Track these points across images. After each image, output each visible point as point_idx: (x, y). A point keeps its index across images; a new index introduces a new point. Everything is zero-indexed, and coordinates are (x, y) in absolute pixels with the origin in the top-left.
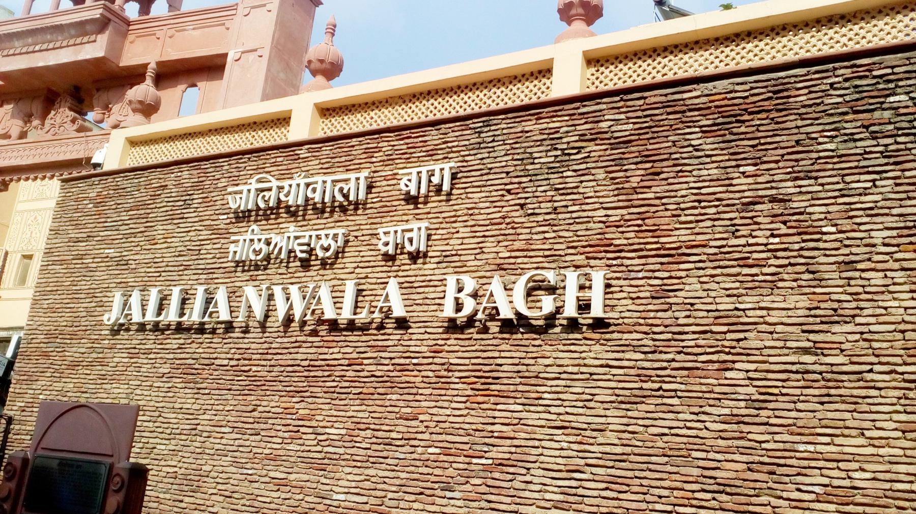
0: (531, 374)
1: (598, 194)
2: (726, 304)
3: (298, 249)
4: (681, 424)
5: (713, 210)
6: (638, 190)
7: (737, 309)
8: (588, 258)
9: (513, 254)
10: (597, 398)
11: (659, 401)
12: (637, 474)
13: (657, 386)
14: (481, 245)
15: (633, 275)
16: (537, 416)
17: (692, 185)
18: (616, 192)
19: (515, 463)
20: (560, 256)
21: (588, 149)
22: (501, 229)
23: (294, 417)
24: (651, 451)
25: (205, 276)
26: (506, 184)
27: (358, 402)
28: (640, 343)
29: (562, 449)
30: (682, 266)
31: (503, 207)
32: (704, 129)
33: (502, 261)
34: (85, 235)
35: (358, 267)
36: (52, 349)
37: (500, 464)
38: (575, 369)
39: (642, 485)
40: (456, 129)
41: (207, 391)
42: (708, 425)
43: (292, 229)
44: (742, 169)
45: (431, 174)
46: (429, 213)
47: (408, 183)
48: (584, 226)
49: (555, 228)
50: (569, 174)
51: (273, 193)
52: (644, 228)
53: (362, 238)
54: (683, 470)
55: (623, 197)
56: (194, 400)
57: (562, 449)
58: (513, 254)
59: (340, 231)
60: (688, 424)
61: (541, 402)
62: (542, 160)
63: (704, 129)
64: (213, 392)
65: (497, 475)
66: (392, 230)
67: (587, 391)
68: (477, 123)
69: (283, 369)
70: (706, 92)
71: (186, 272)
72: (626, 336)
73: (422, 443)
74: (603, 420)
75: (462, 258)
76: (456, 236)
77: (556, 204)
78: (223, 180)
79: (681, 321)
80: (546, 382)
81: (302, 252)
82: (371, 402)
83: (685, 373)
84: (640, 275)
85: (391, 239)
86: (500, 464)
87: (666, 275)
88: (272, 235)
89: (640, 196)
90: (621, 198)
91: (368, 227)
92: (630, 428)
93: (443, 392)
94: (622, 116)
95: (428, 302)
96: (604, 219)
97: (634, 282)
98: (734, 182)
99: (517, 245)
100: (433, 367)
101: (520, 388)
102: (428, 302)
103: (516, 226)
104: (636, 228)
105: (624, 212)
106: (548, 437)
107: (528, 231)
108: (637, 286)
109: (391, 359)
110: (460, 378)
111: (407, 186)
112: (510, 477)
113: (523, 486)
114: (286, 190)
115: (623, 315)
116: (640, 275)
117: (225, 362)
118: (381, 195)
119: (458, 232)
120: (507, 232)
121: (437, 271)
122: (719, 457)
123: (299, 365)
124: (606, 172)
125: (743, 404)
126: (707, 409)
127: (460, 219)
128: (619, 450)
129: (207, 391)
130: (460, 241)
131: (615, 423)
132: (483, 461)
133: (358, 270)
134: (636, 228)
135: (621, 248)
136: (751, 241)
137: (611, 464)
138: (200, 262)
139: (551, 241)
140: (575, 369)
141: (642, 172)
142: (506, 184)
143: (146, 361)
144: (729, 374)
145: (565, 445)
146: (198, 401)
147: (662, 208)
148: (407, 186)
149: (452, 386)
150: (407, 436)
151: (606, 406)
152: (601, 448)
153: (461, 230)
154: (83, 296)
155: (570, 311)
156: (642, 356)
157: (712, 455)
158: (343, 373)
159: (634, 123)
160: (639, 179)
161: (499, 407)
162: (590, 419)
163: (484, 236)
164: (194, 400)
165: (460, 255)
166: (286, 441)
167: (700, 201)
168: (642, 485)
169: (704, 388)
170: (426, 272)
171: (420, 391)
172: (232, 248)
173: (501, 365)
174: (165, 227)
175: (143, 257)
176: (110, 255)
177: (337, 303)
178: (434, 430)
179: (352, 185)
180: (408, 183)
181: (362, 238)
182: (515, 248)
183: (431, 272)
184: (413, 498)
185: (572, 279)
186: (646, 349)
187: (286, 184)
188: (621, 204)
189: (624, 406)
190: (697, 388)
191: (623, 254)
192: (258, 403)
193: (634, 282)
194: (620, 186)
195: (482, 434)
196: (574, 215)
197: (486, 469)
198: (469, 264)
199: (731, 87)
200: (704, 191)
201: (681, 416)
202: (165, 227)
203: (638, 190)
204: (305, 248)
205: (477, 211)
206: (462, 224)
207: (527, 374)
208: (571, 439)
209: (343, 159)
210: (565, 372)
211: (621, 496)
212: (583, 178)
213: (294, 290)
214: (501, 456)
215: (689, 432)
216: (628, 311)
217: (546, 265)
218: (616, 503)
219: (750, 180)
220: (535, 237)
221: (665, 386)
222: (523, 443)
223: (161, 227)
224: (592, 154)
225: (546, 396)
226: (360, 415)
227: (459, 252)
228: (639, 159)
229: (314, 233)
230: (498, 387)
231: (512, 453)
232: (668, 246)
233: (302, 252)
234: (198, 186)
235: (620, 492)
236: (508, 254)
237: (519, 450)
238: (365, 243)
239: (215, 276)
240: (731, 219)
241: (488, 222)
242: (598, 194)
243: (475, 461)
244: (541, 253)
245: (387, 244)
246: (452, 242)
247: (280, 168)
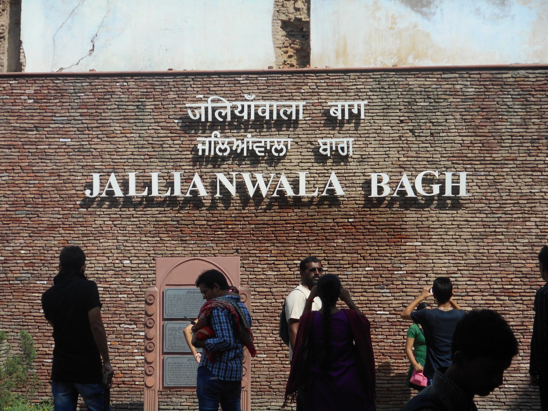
0: (425, 226)
1: (457, 127)
2: (526, 190)
3: (257, 150)
4: (505, 248)
5: (519, 141)
6: (479, 127)
7: (531, 192)
8: (453, 163)
9: (409, 159)
10: (462, 237)
11: (494, 237)
12: (485, 272)
13: (493, 230)
14: (387, 152)
15: (478, 173)
16: (430, 247)
17: (508, 127)
18: (467, 127)
19: (419, 272)
20: (437, 161)
21: (450, 100)
22: (399, 144)
23: (269, 255)
24: (491, 261)
25: (172, 164)
26: (400, 117)
27: (313, 245)
28: (484, 208)
29: (445, 263)
30: (504, 170)
31: (399, 130)
32: (514, 96)
33: (402, 163)
34: (33, 126)
35: (301, 162)
36: (23, 216)
37: (411, 273)
38: (450, 223)
39: (487, 277)
40: (362, 77)
41: (192, 242)
42: (518, 247)
43: (249, 137)
44: (532, 121)
46: (349, 130)
47: (336, 112)
48: (450, 145)
49: (433, 145)
50: (439, 114)
51: (229, 111)
52: (483, 148)
53: (301, 143)
54: (507, 269)
55: (472, 131)
56: (183, 248)
57: (445, 263)
58: (409, 159)
59: (290, 140)
60: (509, 248)
61: (432, 240)
62: (422, 104)
63: (514, 96)
64: (198, 242)
65: (409, 279)
66: (328, 141)
67: (457, 233)
68: (377, 75)
69: (253, 226)
70: (514, 76)
71: (152, 160)
72: (476, 205)
73: (362, 265)
74: (466, 248)
75: (375, 160)
76: (370, 146)
77: (433, 131)
78: (172, 93)
79: (504, 198)
80: (433, 230)
81: (260, 152)
82: (324, 244)
83: (507, 223)
84: (482, 173)
85: (328, 147)
86: (411, 273)
87: (496, 174)
88: (234, 139)
89: (481, 131)
90: (470, 130)
91: (305, 136)
92: (480, 251)
93: (372, 237)
94: (469, 83)
95: (356, 185)
96: (461, 142)
97: (479, 177)
98: (529, 127)
99: (410, 154)
100: (364, 224)
101: (419, 233)
102: (356, 185)
103: (409, 142)
104: (479, 148)
105: (472, 138)
106: (437, 258)
107: (416, 146)
108: (481, 180)
109: (333, 219)
110: (382, 229)
111: (335, 113)
112: (418, 279)
113: (425, 283)
114: (240, 108)
115: (474, 194)
116: (482, 173)
117: (204, 222)
118: (312, 115)
119: (371, 144)
120: (403, 146)
121: (359, 167)
122: (523, 262)
123: (267, 224)
124: (460, 115)
125: (534, 237)
126: (518, 240)
127: (371, 135)
128: (475, 262)
129: (192, 242)
130: (372, 150)
131: (472, 249)
132: (401, 272)
133: (301, 164)
134: (479, 148)
135: (472, 158)
136: (538, 158)
137: (471, 268)
138: (166, 153)
139: (431, 152)
140: (450, 223)
141: (481, 117)
142: (400, 117)
143: (128, 223)
144: (528, 223)
145: (447, 261)
146: (186, 249)
147: (492, 138)
148: (335, 113)
149: (377, 234)
150: (351, 262)
151: (467, 241)
152: (466, 262)
153: (373, 142)
154: (46, 175)
155: (448, 192)
156: (485, 216)
157: (520, 261)
158: (301, 228)
159: (475, 88)
160: (479, 121)
161: (407, 244)
162: (459, 248)
163: (389, 147)
164: (183, 248)
165: (374, 158)
166: (265, 270)
167: (512, 136)
168: (487, 277)
169: (516, 230)
170: (352, 167)
171: (357, 237)
172: (200, 147)
173: (406, 222)
174: (122, 125)
175: (105, 146)
176: (67, 144)
177: (295, 185)
178: (369, 258)
179: (294, 110)
180: (336, 112)
181: (301, 143)
182: (409, 155)
183: (356, 167)
184: (360, 294)
185: (448, 177)
186: (487, 212)
187: (239, 104)
188: (470, 134)
189: (476, 240)
190: (513, 230)
191: (473, 162)
192: (239, 248)
193: (479, 177)
194: (469, 124)
195: (399, 258)
196: (444, 138)
197: (402, 276)
198: (381, 163)
199: (527, 75)
200: (514, 130)
201: (505, 244)
202: (122, 125)
203: (479, 127)
204: (263, 149)
205: (382, 132)
206: (373, 139)
207: (422, 226)
208: (450, 258)
209: (277, 88)
210: (444, 224)
211: (477, 283)
212: (447, 117)
213: (259, 177)
214: (410, 269)
215: (510, 251)
216: (477, 192)
217: (429, 166)
218: (474, 287)
219: (536, 127)
220: (421, 149)
221: (497, 230)
222: (423, 262)
223: (118, 125)
224: (453, 104)
225: (434, 237)
226: (317, 252)
227: (374, 156)
228: (479, 109)
229: (268, 140)
230: (406, 233)
231: (417, 267)
232: (496, 159)
233: (260, 152)
234: (146, 95)
235: (476, 281)
236: (406, 159)
237: (421, 265)
238: (304, 147)
239: (181, 164)
240: (527, 147)
241: (391, 139)
242: (457, 127)
243: (396, 272)
244: (426, 159)
245: (325, 150)
246: (367, 149)
247: (224, 89)
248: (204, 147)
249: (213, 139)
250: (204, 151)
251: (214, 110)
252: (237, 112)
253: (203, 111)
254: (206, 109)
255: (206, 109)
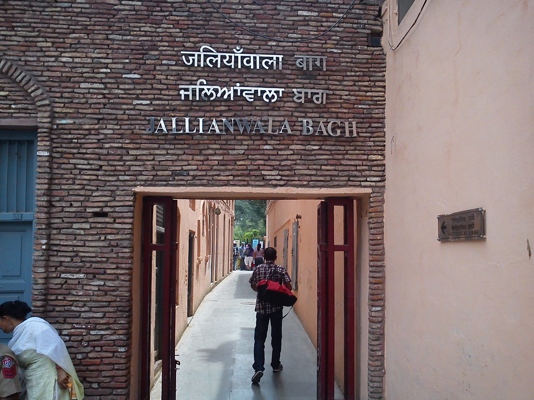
45: (315, 60)
51: (219, 59)
248: (186, 93)
249: (198, 87)
250: (187, 96)
251: (206, 57)
252: (225, 61)
253: (196, 58)
254: (199, 56)
255: (199, 56)
